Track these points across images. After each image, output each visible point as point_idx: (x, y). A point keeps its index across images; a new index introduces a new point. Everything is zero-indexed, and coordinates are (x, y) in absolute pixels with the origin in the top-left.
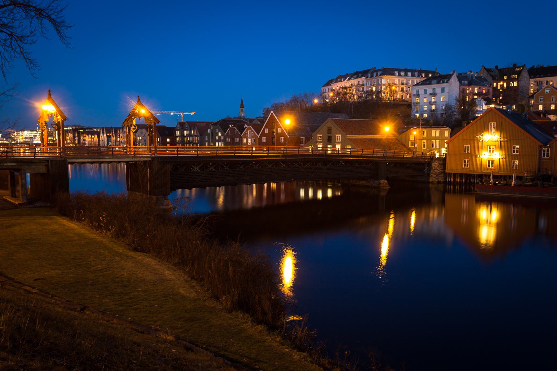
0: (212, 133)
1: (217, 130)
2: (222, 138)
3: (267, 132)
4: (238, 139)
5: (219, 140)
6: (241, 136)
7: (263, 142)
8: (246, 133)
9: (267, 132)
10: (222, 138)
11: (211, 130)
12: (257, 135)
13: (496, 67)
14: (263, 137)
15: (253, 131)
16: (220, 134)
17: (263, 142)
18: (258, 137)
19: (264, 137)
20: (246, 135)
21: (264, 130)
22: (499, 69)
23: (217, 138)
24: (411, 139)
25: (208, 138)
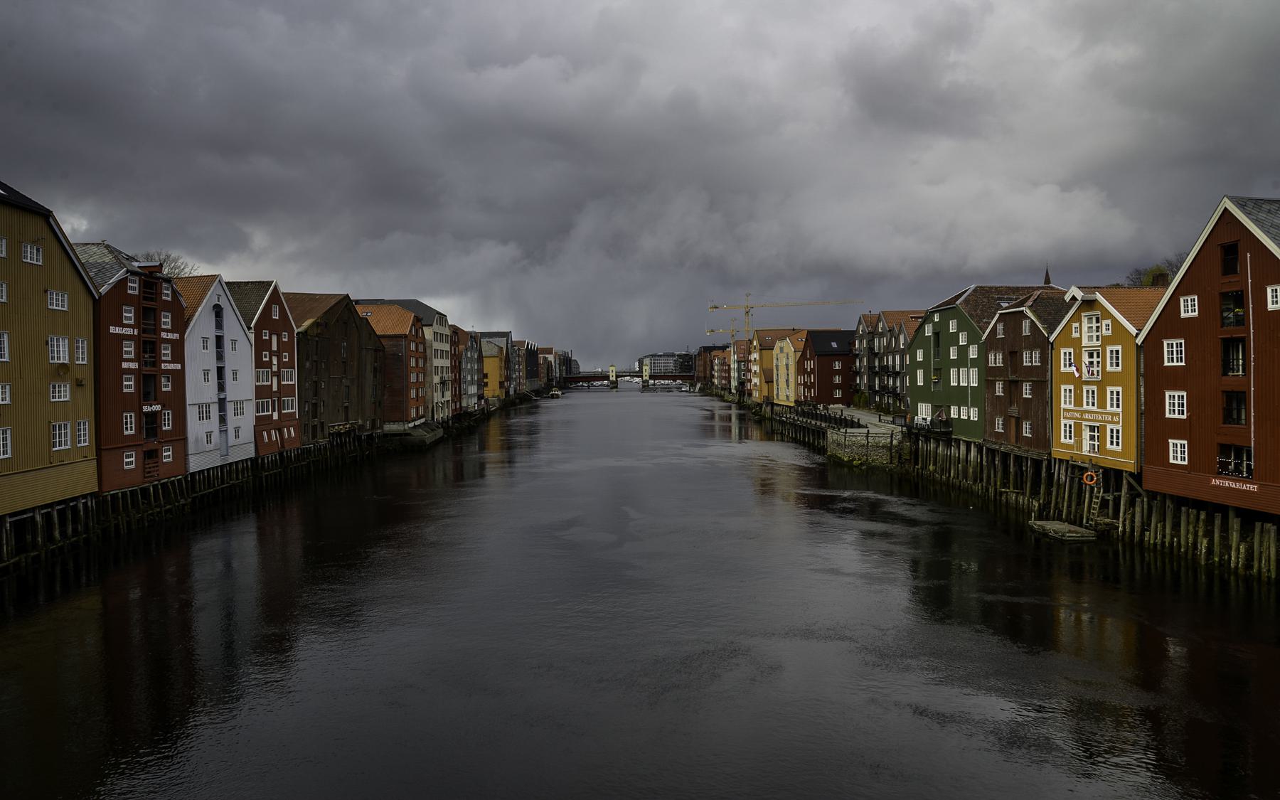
0: (936, 334)
1: (953, 326)
2: (973, 353)
3: (1196, 314)
4: (1036, 354)
5: (962, 361)
6: (1051, 339)
9: (1196, 314)
10: (973, 353)
11: (935, 324)
12: (1133, 331)
15: (1110, 316)
17: (1166, 364)
18: (1139, 341)
21: (1173, 303)
25: (926, 355)
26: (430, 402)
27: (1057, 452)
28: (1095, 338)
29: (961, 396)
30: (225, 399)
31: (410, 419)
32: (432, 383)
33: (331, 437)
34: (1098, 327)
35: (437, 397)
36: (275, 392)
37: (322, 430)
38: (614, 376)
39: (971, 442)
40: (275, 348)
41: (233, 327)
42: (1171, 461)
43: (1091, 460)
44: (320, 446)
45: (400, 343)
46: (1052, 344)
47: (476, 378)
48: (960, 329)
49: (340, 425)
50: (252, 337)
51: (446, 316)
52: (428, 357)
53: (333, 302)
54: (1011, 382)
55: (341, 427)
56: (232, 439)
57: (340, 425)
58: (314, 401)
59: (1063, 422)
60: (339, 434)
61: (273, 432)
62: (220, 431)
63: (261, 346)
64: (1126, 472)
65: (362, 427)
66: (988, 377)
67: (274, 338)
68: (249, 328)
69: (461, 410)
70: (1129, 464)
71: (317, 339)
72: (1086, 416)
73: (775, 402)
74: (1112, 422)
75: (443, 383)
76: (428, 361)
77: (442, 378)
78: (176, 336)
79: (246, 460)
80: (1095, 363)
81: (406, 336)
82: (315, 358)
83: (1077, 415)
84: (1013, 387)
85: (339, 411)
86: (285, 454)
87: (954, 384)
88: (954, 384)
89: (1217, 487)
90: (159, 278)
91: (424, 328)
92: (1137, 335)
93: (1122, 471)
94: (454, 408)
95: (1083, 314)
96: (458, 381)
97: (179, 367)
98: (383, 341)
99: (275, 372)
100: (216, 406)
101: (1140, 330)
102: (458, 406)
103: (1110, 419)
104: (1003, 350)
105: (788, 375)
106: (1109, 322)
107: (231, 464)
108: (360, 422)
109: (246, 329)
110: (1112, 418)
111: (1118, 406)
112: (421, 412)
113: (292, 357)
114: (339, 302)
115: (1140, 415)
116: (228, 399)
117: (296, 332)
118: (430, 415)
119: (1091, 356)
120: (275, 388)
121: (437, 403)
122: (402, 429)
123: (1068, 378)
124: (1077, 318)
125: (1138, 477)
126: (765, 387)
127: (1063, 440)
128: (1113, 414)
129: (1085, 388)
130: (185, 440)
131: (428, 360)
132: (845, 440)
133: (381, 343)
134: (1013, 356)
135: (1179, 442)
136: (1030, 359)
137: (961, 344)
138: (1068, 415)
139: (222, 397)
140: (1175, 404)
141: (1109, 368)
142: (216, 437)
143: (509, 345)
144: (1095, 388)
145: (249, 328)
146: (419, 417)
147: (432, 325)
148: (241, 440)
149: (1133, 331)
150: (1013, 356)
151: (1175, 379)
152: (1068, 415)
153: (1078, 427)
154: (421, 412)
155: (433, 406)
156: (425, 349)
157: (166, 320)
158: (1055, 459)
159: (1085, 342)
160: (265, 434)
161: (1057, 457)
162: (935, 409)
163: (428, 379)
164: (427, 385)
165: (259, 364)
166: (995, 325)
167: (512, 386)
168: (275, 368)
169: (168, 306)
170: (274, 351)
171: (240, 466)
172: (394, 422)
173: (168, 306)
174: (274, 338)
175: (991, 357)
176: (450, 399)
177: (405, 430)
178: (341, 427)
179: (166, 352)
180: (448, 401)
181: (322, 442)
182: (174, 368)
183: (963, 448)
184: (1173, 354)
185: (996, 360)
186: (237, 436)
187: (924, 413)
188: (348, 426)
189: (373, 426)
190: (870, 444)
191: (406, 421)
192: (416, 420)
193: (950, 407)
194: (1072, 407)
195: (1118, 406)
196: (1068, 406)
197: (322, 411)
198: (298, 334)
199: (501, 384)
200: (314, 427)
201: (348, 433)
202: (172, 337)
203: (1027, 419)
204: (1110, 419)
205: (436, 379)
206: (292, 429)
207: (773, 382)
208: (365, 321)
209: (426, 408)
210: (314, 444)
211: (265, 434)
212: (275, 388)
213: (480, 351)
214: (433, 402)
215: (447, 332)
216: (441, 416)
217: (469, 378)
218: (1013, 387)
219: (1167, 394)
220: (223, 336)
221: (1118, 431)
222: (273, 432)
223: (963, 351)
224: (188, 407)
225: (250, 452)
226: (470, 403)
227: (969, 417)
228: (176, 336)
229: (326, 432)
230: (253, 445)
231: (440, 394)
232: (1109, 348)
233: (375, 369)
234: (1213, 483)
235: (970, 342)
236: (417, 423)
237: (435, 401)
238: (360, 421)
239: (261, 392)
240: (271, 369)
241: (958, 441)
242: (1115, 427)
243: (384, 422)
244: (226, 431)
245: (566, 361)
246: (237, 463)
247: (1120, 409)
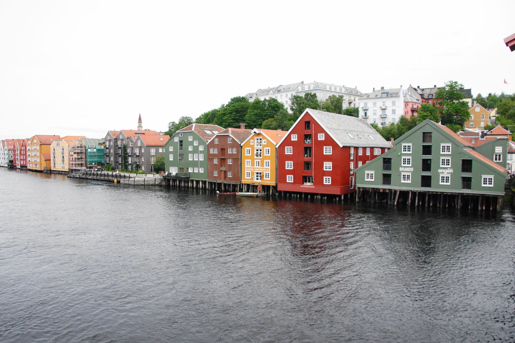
0: (181, 141)
3: (296, 140)
7: (286, 153)
9: (296, 140)
10: (201, 148)
11: (180, 137)
13: (418, 87)
14: (286, 147)
16: (196, 144)
17: (286, 153)
18: (277, 147)
19: (289, 147)
21: (289, 136)
22: (421, 89)
23: (190, 149)
24: (496, 152)
27: (244, 181)
39: (199, 181)
42: (288, 181)
46: (242, 147)
48: (194, 139)
59: (246, 171)
70: (273, 183)
73: (52, 169)
83: (252, 169)
84: (223, 161)
95: (255, 137)
105: (63, 157)
106: (265, 140)
111: (268, 166)
115: (276, 169)
119: (257, 150)
123: (248, 158)
124: (252, 138)
125: (275, 188)
127: (246, 177)
128: (266, 169)
129: (255, 161)
134: (223, 150)
135: (290, 176)
137: (195, 145)
140: (289, 165)
141: (265, 155)
149: (275, 144)
150: (223, 150)
151: (289, 158)
152: (248, 169)
153: (253, 173)
158: (243, 184)
159: (256, 146)
161: (244, 183)
162: (181, 169)
166: (214, 139)
183: (195, 183)
184: (289, 151)
187: (174, 171)
194: (250, 166)
195: (268, 166)
196: (248, 166)
203: (230, 171)
218: (223, 161)
219: (286, 162)
221: (268, 174)
227: (199, 171)
232: (265, 148)
242: (267, 173)
247: (269, 167)
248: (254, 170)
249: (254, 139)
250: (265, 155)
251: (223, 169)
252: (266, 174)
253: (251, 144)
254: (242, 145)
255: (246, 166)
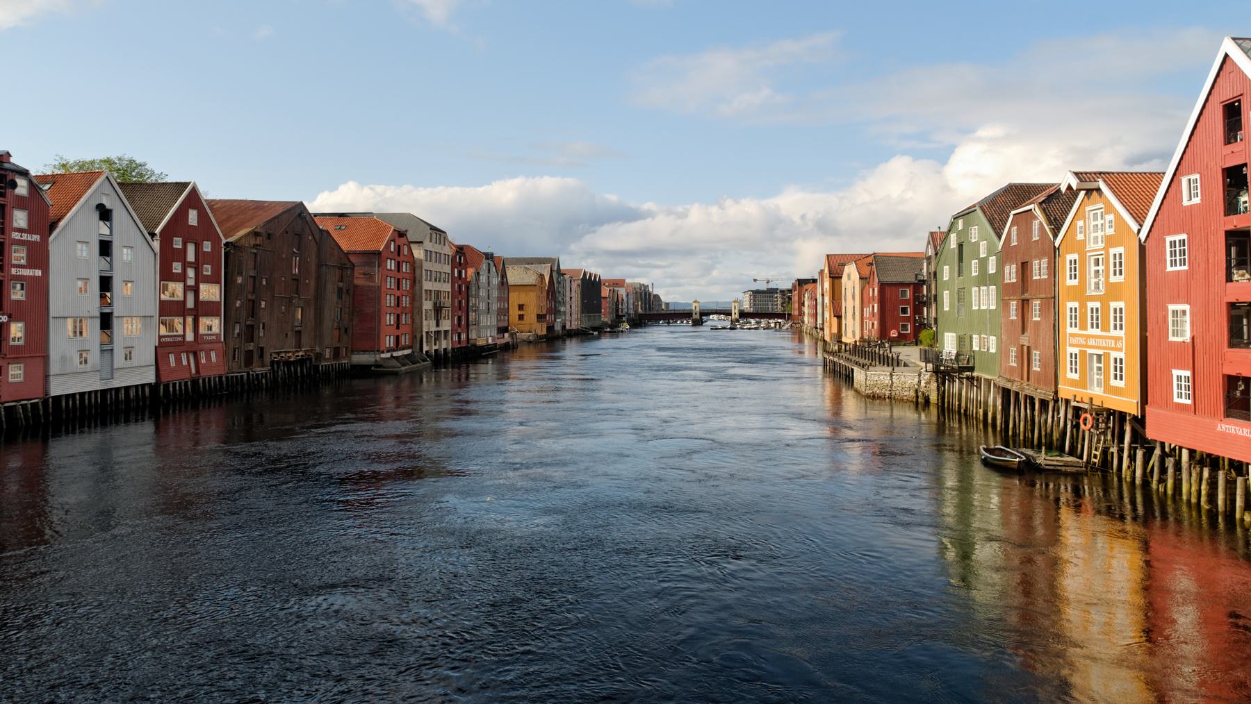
0: (960, 246)
5: (984, 279)
8: (1080, 223)
10: (992, 269)
17: (1169, 269)
19: (1177, 238)
20: (1080, 237)
26: (419, 330)
27: (1065, 391)
28: (1100, 240)
29: (983, 321)
30: (112, 313)
31: (382, 349)
32: (421, 309)
33: (275, 366)
34: (1102, 225)
35: (429, 325)
36: (191, 309)
37: (261, 356)
38: (698, 314)
40: (191, 257)
41: (125, 229)
42: (1176, 400)
43: (1091, 399)
44: (257, 375)
45: (373, 260)
47: (494, 307)
48: (982, 238)
49: (289, 352)
50: (156, 245)
51: (445, 233)
52: (417, 279)
53: (281, 210)
54: (1023, 300)
55: (290, 354)
56: (119, 360)
57: (289, 352)
58: (248, 323)
59: (1070, 350)
60: (288, 363)
61: (184, 357)
62: (102, 351)
63: (168, 257)
64: (1130, 414)
65: (319, 356)
66: (1005, 292)
67: (191, 249)
68: (153, 235)
69: (468, 343)
70: (1129, 404)
71: (255, 251)
72: (1091, 342)
74: (1116, 349)
75: (438, 309)
76: (417, 284)
77: (435, 304)
78: (36, 238)
79: (143, 386)
80: (1101, 272)
81: (379, 253)
82: (252, 273)
85: (287, 335)
86: (201, 381)
87: (975, 308)
88: (975, 308)
89: (1224, 435)
90: (6, 170)
91: (413, 246)
92: (1139, 231)
93: (1126, 413)
94: (456, 338)
95: (1087, 209)
96: (465, 309)
97: (38, 273)
98: (353, 259)
99: (190, 286)
100: (97, 322)
101: (1141, 226)
102: (463, 336)
103: (1113, 345)
104: (1016, 261)
107: (117, 390)
108: (318, 349)
109: (149, 238)
110: (1116, 344)
112: (405, 340)
113: (216, 271)
114: (289, 210)
116: (115, 314)
117: (224, 241)
118: (418, 345)
120: (190, 304)
121: (427, 333)
122: (373, 360)
126: (835, 320)
130: (46, 358)
131: (417, 282)
132: (866, 379)
133: (349, 260)
134: (1024, 267)
136: (1039, 270)
137: (981, 256)
138: (1074, 341)
139: (107, 310)
142: (94, 357)
143: (555, 275)
144: (1097, 305)
145: (153, 235)
146: (398, 346)
147: (422, 242)
148: (135, 361)
150: (1024, 267)
152: (1074, 341)
154: (405, 340)
155: (422, 336)
156: (413, 269)
157: (20, 218)
160: (172, 358)
163: (416, 304)
164: (416, 311)
165: (166, 275)
167: (558, 320)
168: (191, 282)
169: (21, 203)
170: (190, 263)
171: (132, 393)
172: (365, 351)
173: (21, 203)
174: (191, 249)
175: (1007, 268)
176: (449, 328)
177: (376, 361)
178: (290, 354)
179: (18, 256)
180: (446, 332)
181: (259, 370)
182: (31, 274)
185: (1011, 274)
186: (128, 357)
188: (300, 354)
189: (336, 353)
190: (895, 385)
191: (378, 351)
192: (394, 350)
193: (971, 338)
197: (261, 334)
198: (227, 244)
199: (540, 317)
200: (249, 354)
201: (301, 362)
202: (29, 239)
204: (1113, 345)
205: (428, 305)
206: (213, 355)
207: (841, 317)
208: (325, 234)
209: (414, 337)
210: (248, 373)
211: (172, 358)
212: (190, 304)
213: (504, 276)
214: (422, 331)
215: (448, 251)
216: (435, 348)
217: (483, 306)
220: (111, 242)
222: (184, 357)
223: (983, 263)
224: (51, 320)
225: (150, 378)
226: (485, 335)
227: (988, 350)
228: (36, 238)
229: (267, 359)
230: (153, 369)
231: (433, 322)
232: (1112, 251)
233: (340, 290)
234: (1219, 429)
235: (989, 254)
236: (395, 354)
237: (425, 330)
238: (317, 348)
239: (168, 309)
240: (184, 281)
241: (979, 379)
243: (352, 352)
244: (112, 350)
245: (645, 296)
246: (127, 389)
248: (1087, 346)
249: (1084, 218)
250: (1113, 279)
251: (1024, 340)
252: (1116, 359)
253: (1080, 237)
254: (1057, 245)
255: (1070, 330)
